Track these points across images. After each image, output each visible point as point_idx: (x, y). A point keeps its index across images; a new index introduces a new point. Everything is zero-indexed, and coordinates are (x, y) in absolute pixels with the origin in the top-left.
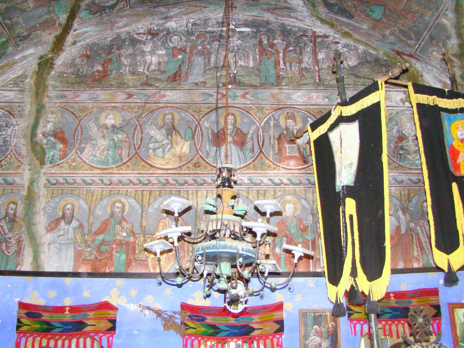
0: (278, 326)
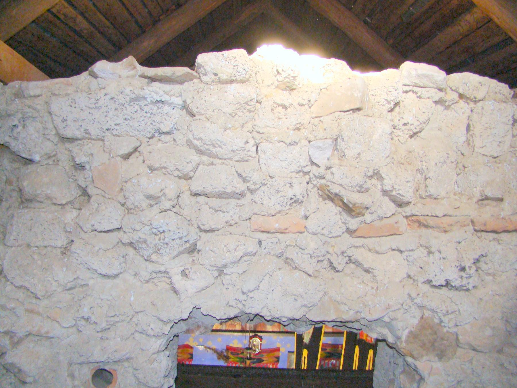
0: (276, 360)
